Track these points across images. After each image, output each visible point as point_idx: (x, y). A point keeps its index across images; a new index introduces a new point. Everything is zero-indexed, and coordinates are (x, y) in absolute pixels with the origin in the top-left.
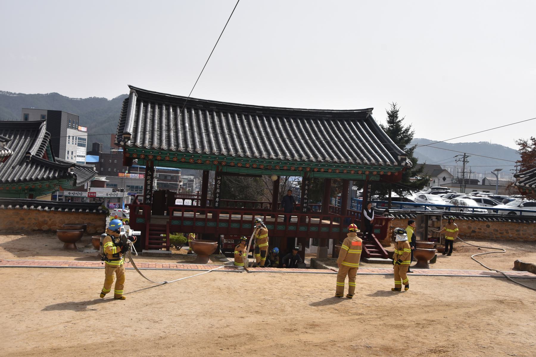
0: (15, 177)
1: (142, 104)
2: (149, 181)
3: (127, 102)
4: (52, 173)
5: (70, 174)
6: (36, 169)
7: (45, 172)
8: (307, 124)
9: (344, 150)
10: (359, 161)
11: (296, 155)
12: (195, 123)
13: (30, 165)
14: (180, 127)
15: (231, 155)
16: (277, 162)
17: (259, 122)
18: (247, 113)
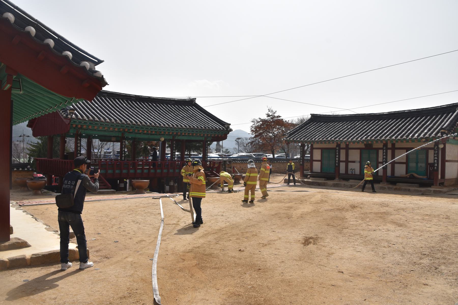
2: (79, 144)
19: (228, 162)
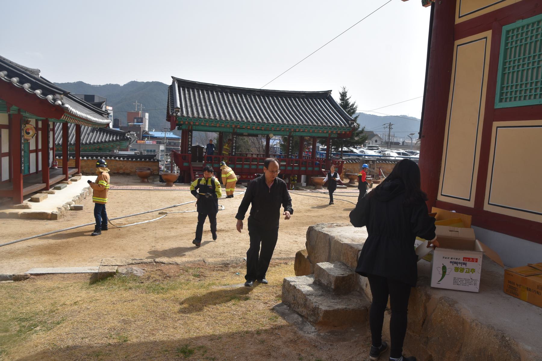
0: (94, 140)
1: (181, 88)
3: (172, 88)
4: (115, 137)
5: (127, 137)
6: (103, 135)
7: (110, 137)
8: (289, 101)
9: (315, 118)
10: (325, 124)
11: (285, 121)
12: (217, 101)
13: (99, 132)
14: (208, 103)
15: (244, 121)
16: (273, 125)
17: (258, 99)
18: (249, 94)
19: (371, 162)
